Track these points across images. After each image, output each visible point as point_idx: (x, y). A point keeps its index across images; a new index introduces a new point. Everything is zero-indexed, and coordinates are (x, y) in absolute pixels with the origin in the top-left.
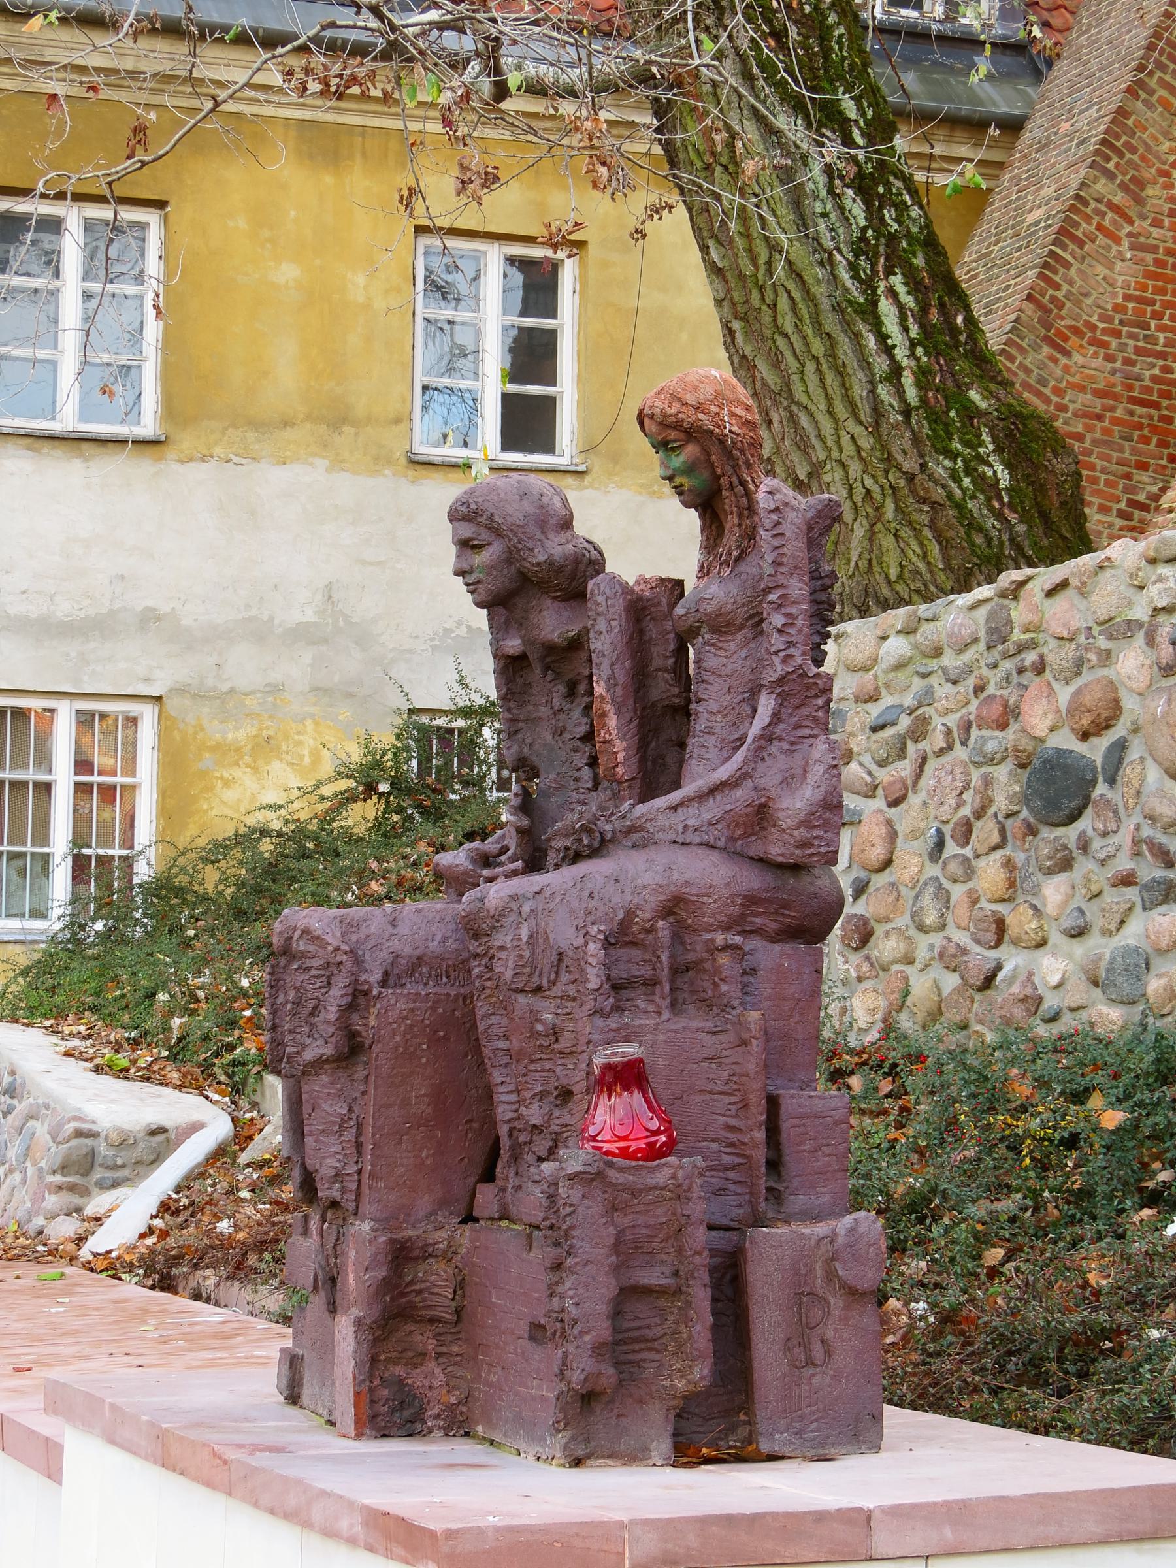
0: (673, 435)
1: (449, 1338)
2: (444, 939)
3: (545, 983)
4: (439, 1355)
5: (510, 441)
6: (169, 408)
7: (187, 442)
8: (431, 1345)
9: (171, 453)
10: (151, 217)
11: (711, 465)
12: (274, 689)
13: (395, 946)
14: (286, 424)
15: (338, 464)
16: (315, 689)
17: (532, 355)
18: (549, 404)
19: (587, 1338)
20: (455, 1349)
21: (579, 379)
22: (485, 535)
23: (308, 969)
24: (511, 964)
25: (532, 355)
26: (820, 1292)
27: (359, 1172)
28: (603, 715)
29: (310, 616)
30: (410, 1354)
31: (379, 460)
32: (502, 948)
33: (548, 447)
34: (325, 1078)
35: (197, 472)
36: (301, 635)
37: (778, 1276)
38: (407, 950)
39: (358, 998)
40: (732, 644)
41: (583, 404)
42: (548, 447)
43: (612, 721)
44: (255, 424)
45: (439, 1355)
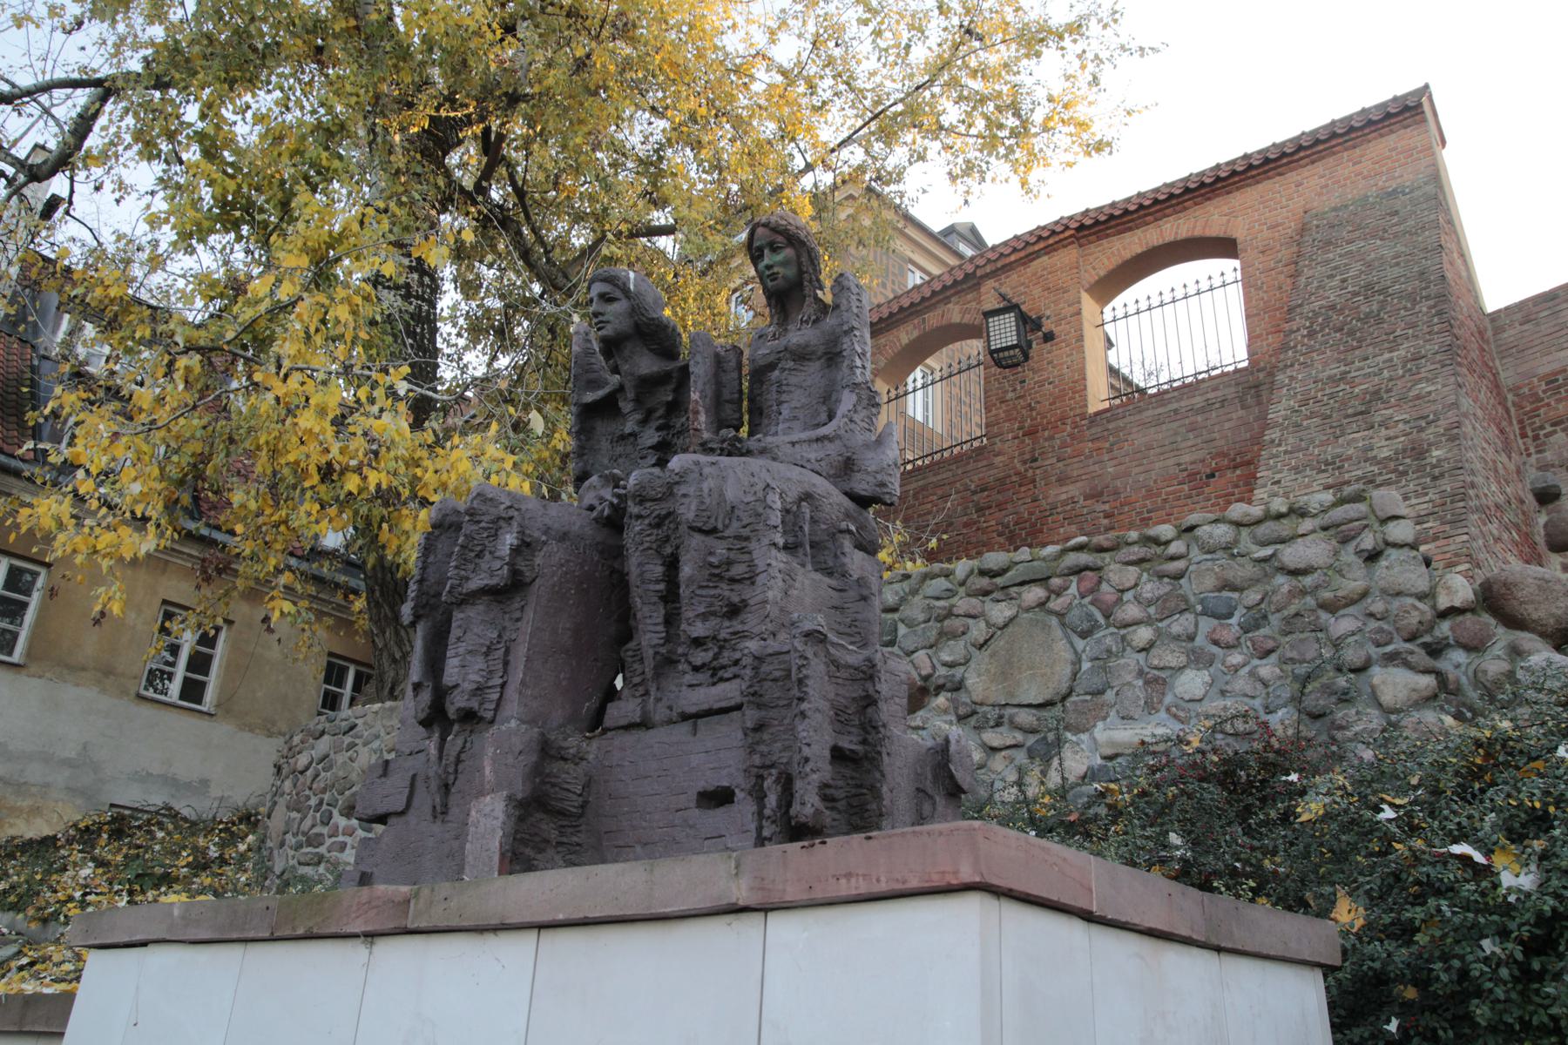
0: (780, 238)
1: (570, 830)
2: (582, 527)
3: (720, 526)
4: (560, 844)
5: (184, 695)
6: (29, 653)
7: (33, 669)
8: (554, 836)
9: (24, 672)
10: (43, 572)
11: (800, 264)
12: (47, 785)
13: (547, 521)
14: (84, 669)
15: (103, 691)
16: (68, 788)
17: (200, 663)
18: (203, 685)
19: (815, 776)
20: (575, 839)
21: (218, 676)
22: (618, 294)
23: (479, 522)
24: (693, 507)
25: (200, 663)
26: (930, 791)
27: (503, 686)
28: (697, 413)
29: (73, 755)
30: (537, 839)
31: (124, 692)
32: (685, 496)
33: (200, 703)
34: (481, 608)
35: (35, 682)
36: (67, 763)
37: (905, 771)
38: (556, 526)
39: (525, 547)
40: (814, 367)
41: (222, 688)
42: (199, 701)
43: (702, 418)
44: (68, 667)
45: (560, 844)
